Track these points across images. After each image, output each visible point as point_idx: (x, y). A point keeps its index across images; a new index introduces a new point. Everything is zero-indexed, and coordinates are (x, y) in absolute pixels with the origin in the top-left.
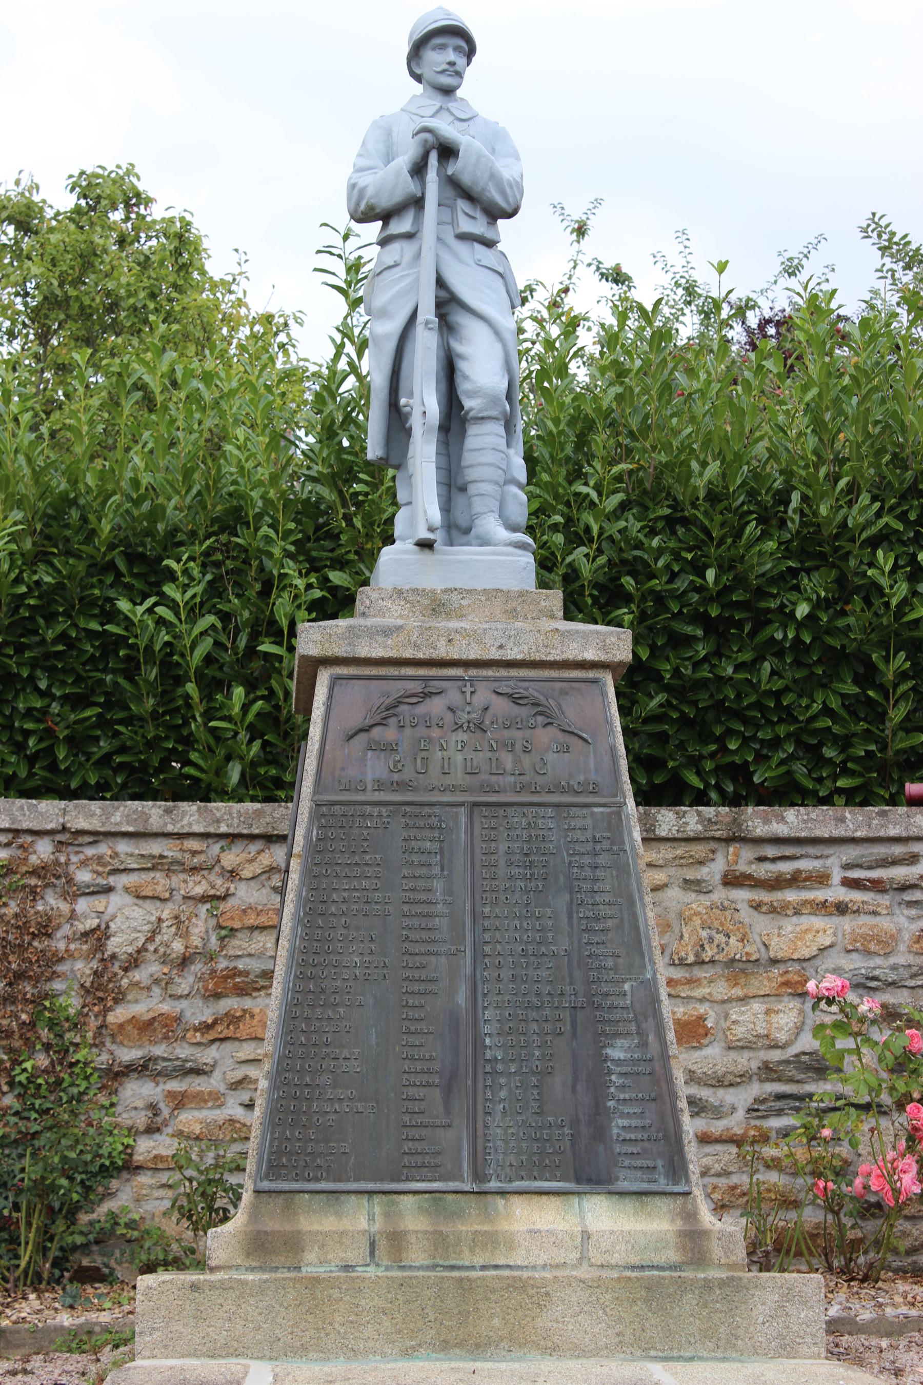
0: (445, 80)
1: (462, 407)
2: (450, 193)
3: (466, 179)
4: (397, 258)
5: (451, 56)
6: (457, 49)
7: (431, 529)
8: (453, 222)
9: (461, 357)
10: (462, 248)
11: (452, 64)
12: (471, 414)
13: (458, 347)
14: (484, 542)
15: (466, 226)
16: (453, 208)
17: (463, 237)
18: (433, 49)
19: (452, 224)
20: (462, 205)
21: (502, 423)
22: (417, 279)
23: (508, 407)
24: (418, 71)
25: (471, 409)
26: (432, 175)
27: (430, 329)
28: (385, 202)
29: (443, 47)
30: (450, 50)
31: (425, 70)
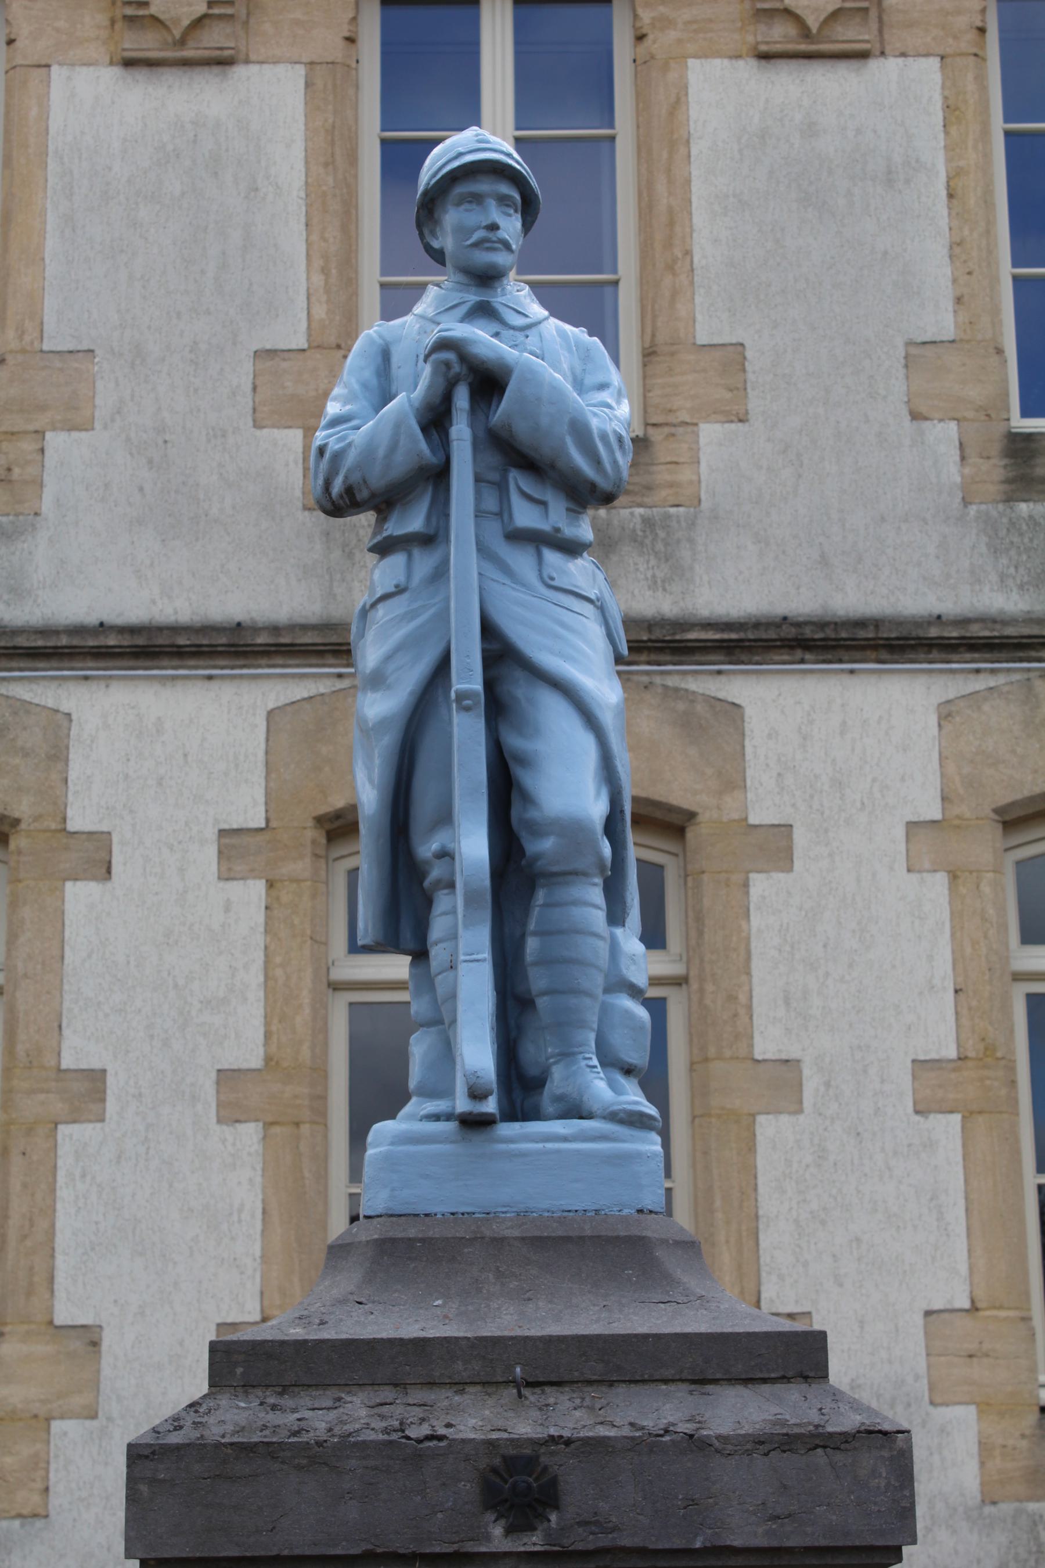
0: (483, 258)
1: (522, 851)
2: (493, 459)
3: (522, 430)
4: (402, 579)
6: (503, 200)
7: (476, 1094)
8: (504, 512)
9: (524, 761)
10: (522, 560)
13: (513, 741)
14: (575, 1110)
15: (525, 516)
16: (502, 488)
17: (519, 537)
18: (459, 204)
19: (499, 514)
20: (517, 479)
21: (599, 880)
22: (443, 616)
24: (436, 244)
26: (461, 431)
27: (467, 709)
28: (378, 479)
29: (477, 199)
30: (492, 204)
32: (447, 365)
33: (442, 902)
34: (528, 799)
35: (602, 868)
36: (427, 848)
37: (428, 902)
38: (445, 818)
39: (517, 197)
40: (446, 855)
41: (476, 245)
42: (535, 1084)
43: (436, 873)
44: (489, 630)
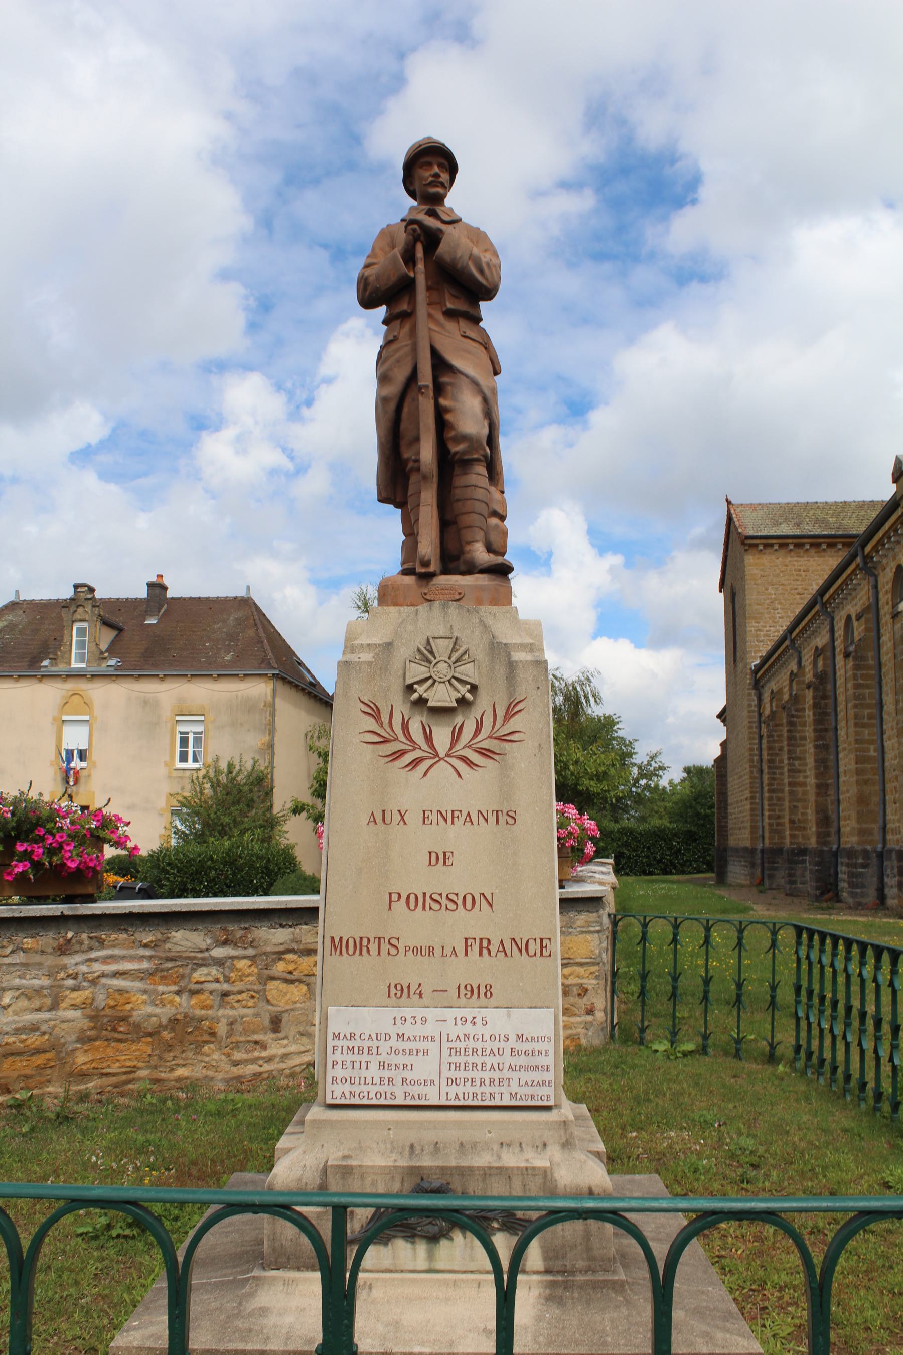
5: (436, 169)
6: (440, 165)
8: (441, 303)
11: (437, 176)
12: (457, 457)
18: (421, 167)
23: (488, 450)
24: (412, 188)
25: (456, 453)
29: (430, 165)
31: (417, 187)
32: (414, 230)
33: (414, 478)
34: (451, 427)
35: (485, 456)
36: (407, 454)
37: (408, 479)
38: (417, 439)
39: (446, 163)
40: (417, 461)
41: (431, 184)
42: (456, 558)
43: (411, 465)
44: (435, 353)
